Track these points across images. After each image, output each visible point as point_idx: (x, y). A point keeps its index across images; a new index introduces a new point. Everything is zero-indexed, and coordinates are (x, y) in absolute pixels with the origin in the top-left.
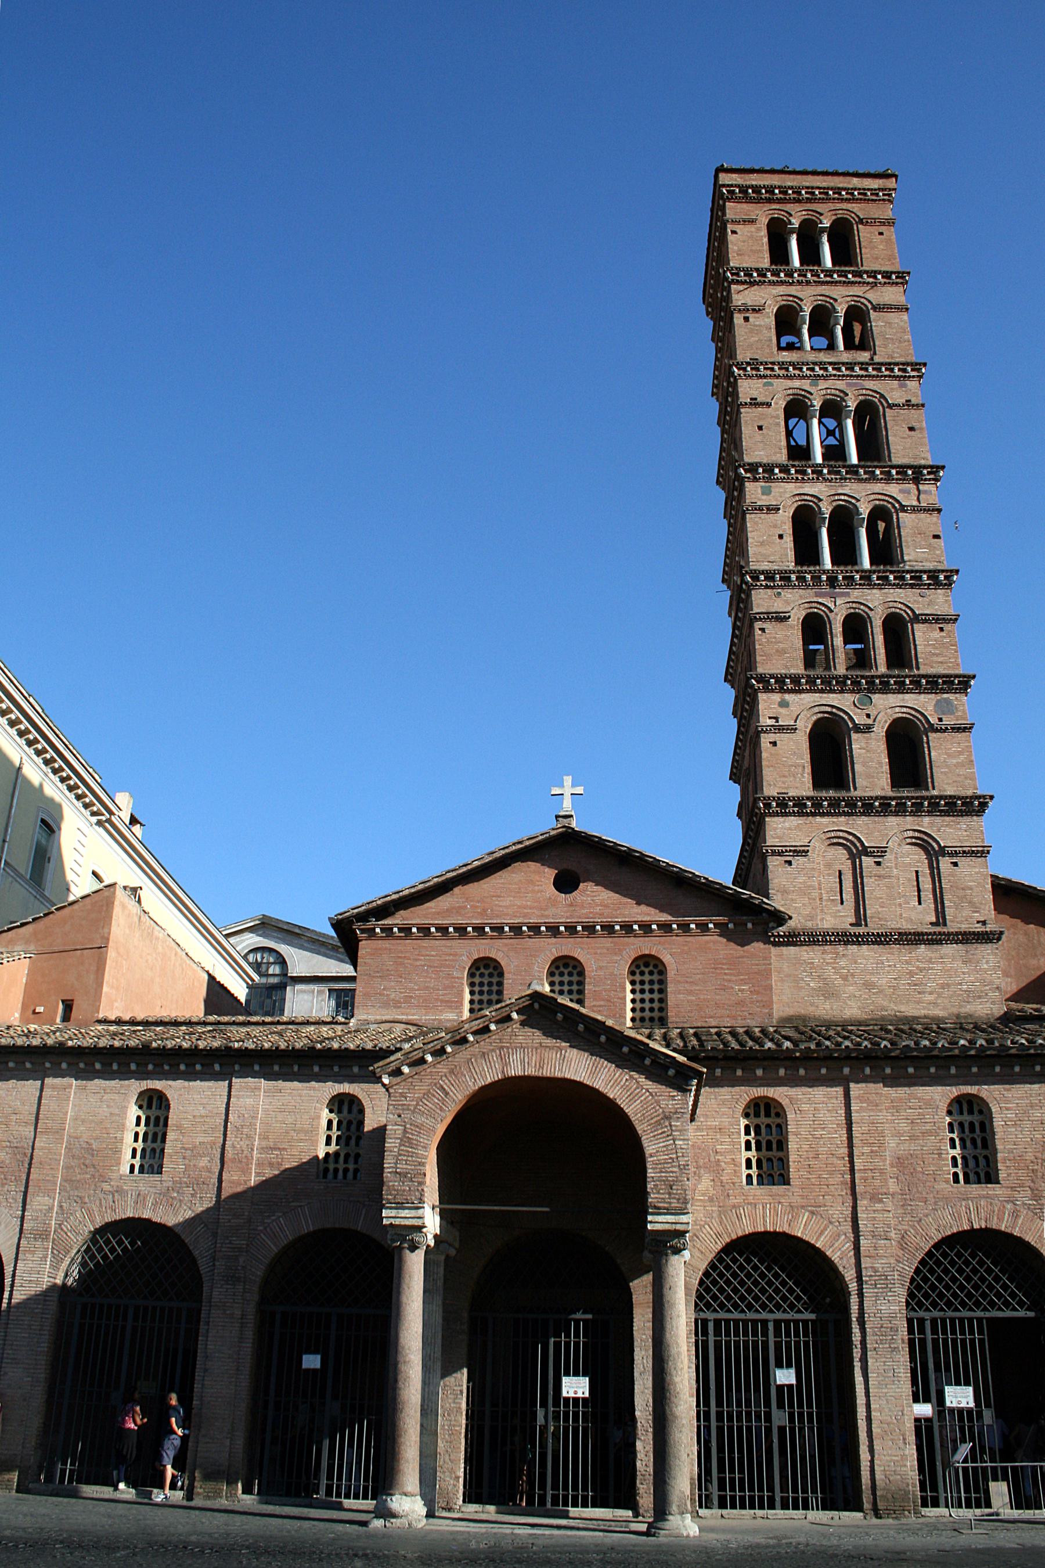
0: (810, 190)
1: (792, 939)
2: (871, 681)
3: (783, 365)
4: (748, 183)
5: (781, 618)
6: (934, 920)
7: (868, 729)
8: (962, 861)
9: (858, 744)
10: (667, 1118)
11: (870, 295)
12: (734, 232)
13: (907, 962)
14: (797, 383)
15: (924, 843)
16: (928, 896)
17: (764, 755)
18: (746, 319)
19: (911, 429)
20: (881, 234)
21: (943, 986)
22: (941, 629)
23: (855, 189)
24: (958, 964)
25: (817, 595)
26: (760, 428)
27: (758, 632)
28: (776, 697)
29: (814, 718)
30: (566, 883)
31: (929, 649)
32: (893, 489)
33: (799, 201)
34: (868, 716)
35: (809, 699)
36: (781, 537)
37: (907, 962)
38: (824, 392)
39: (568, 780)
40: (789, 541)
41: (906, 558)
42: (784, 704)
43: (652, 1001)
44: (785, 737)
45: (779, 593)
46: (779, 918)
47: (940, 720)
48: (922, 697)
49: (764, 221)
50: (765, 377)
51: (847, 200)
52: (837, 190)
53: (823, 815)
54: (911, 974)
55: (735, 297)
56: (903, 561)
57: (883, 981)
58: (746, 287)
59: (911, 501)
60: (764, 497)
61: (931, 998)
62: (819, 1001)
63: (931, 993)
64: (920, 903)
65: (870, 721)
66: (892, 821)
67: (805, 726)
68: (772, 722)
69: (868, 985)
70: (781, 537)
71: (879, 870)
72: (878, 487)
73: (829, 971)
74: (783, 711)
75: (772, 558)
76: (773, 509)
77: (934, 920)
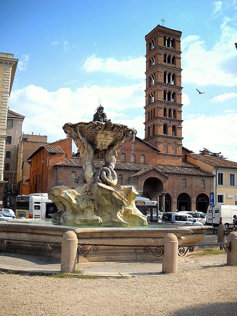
1: (160, 154)
2: (171, 119)
3: (165, 65)
18: (160, 55)
32: (176, 90)
42: (161, 121)
46: (159, 151)
48: (177, 123)
52: (174, 34)
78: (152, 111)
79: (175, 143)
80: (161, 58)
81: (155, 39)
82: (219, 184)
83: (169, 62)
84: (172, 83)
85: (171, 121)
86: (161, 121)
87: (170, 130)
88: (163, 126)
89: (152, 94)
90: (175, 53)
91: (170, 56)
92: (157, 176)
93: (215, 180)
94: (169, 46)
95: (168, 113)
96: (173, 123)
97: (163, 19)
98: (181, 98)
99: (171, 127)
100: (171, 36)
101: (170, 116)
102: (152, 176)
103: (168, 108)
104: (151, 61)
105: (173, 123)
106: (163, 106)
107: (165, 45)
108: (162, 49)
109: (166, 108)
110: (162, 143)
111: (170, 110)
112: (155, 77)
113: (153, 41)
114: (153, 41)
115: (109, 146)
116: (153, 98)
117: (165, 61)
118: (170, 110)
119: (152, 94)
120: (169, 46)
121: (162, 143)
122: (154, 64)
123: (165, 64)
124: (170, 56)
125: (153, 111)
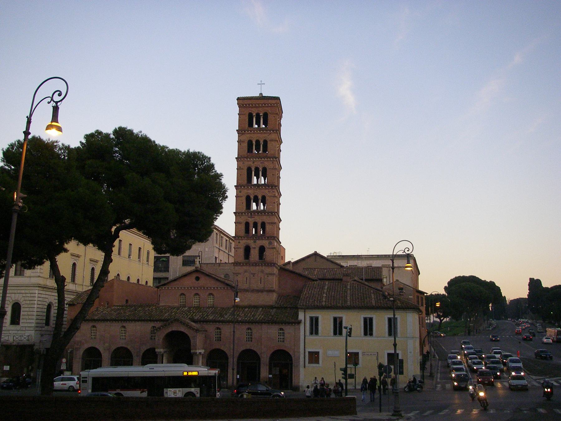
0: (259, 104)
4: (244, 103)
7: (254, 248)
9: (252, 251)
10: (194, 337)
14: (249, 163)
19: (273, 175)
22: (272, 225)
23: (269, 104)
25: (249, 217)
26: (241, 175)
28: (238, 241)
29: (245, 245)
30: (197, 279)
32: (267, 191)
33: (255, 107)
34: (255, 245)
35: (244, 241)
38: (255, 165)
42: (239, 242)
43: (212, 301)
44: (239, 249)
45: (241, 217)
47: (269, 246)
48: (266, 241)
50: (243, 161)
51: (268, 107)
53: (244, 266)
58: (241, 134)
60: (240, 193)
64: (261, 284)
65: (255, 247)
66: (257, 267)
71: (254, 277)
72: (263, 191)
74: (239, 244)
76: (241, 197)
79: (262, 272)
82: (311, 333)
86: (239, 242)
87: (254, 254)
91: (258, 142)
92: (182, 329)
93: (304, 328)
96: (260, 243)
99: (257, 249)
100: (260, 109)
102: (174, 329)
103: (251, 221)
105: (260, 243)
108: (243, 134)
109: (249, 221)
110: (240, 274)
121: (240, 274)
124: (258, 142)
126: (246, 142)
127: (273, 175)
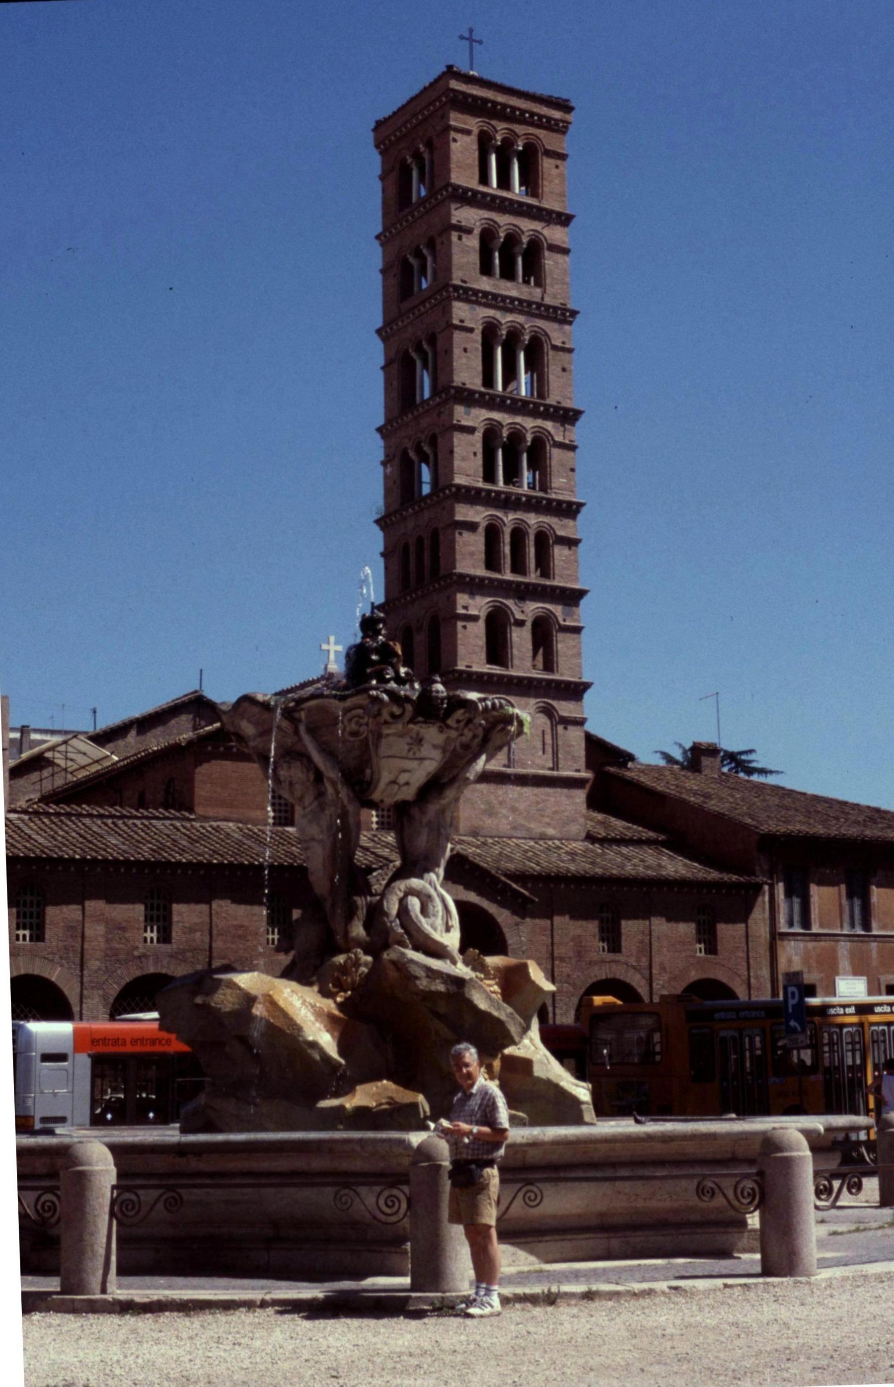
5: (472, 527)
6: (551, 765)
7: (520, 623)
8: (570, 728)
11: (546, 232)
12: (455, 140)
13: (536, 795)
15: (548, 711)
16: (549, 750)
17: (459, 636)
18: (460, 238)
19: (564, 370)
20: (557, 167)
21: (555, 812)
24: (563, 798)
26: (465, 350)
27: (457, 535)
31: (562, 563)
36: (475, 454)
37: (536, 795)
39: (332, 639)
40: (480, 456)
41: (553, 485)
47: (564, 620)
49: (476, 131)
54: (538, 803)
55: (453, 212)
56: (551, 489)
57: (522, 806)
59: (559, 438)
61: (547, 820)
62: (485, 818)
63: (548, 817)
67: (483, 615)
68: (463, 611)
69: (514, 809)
70: (475, 454)
73: (492, 798)
75: (469, 473)
77: (551, 765)
78: (420, 540)
80: (465, 251)
81: (429, 145)
83: (508, 274)
84: (523, 386)
85: (524, 593)
88: (481, 624)
89: (419, 450)
90: (537, 226)
94: (505, 182)
95: (507, 549)
97: (471, 31)
98: (573, 470)
99: (529, 625)
101: (518, 566)
104: (411, 266)
106: (479, 514)
107: (484, 179)
111: (518, 535)
112: (435, 354)
113: (417, 156)
114: (417, 156)
115: (369, 783)
116: (425, 469)
117: (486, 269)
118: (518, 535)
119: (419, 450)
120: (505, 182)
122: (424, 285)
123: (485, 284)
125: (427, 542)
126: (477, 232)
127: (564, 370)
